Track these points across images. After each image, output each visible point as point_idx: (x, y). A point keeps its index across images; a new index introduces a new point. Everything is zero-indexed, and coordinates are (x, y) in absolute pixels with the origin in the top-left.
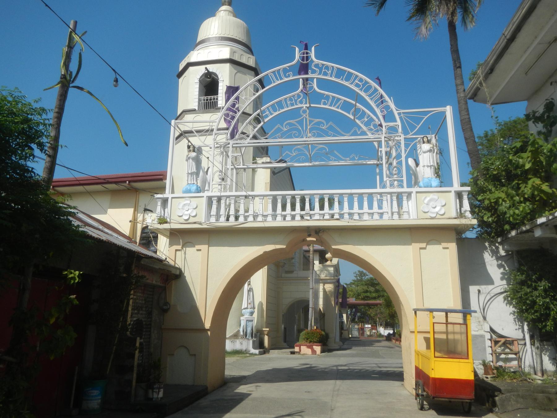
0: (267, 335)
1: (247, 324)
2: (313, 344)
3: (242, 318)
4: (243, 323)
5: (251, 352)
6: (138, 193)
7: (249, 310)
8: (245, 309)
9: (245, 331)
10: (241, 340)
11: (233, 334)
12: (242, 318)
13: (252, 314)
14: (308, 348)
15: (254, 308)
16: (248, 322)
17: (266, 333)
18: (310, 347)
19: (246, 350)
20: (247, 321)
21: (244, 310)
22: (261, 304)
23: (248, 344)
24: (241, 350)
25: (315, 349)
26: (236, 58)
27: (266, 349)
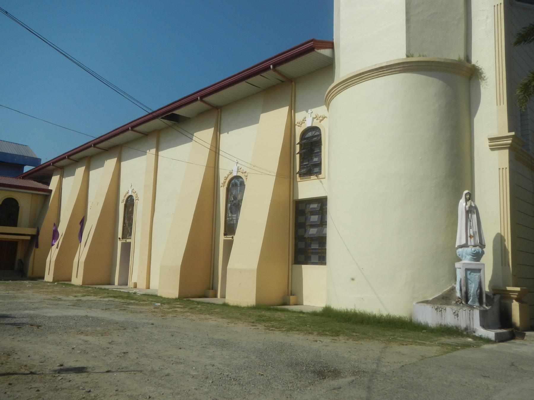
0: (517, 300)
1: (469, 277)
3: (457, 265)
4: (460, 274)
5: (478, 334)
6: (293, 83)
7: (470, 250)
8: (461, 247)
9: (464, 289)
10: (455, 308)
11: (440, 294)
12: (457, 265)
13: (477, 256)
15: (482, 245)
16: (469, 272)
17: (514, 296)
19: (466, 329)
20: (467, 270)
22: (499, 239)
23: (471, 318)
24: (457, 328)
27: (517, 328)
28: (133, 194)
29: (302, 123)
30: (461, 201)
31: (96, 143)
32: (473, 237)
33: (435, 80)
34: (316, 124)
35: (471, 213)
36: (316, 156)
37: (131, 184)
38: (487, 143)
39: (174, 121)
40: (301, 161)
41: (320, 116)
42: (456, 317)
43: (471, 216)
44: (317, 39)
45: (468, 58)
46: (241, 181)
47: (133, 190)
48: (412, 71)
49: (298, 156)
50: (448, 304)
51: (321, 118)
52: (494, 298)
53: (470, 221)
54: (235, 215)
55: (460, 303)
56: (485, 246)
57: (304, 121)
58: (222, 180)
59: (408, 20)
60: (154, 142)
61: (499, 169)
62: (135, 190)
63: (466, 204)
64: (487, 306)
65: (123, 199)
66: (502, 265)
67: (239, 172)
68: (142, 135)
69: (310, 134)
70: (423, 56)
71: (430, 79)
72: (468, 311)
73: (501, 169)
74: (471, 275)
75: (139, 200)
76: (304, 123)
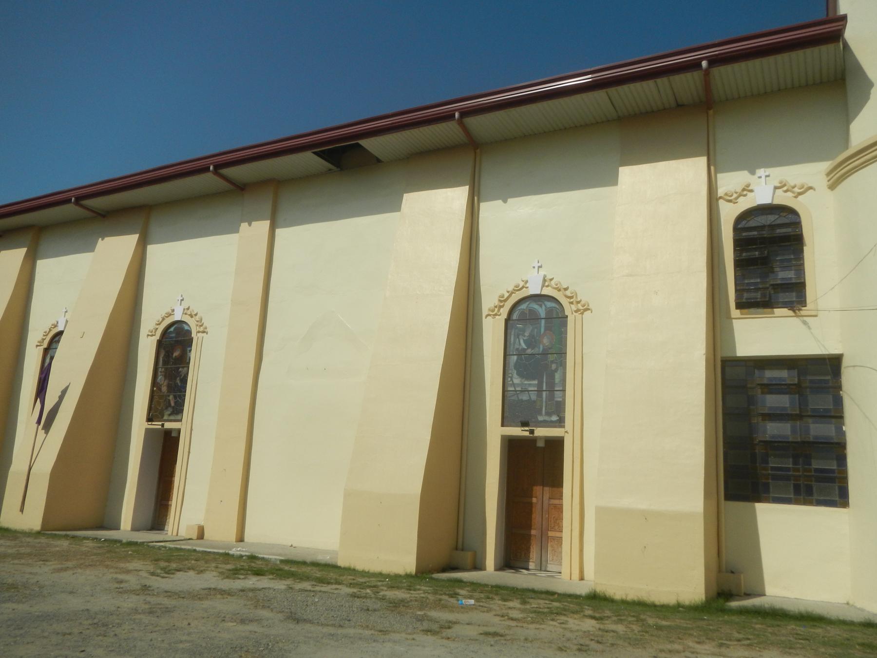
28: (186, 319)
29: (740, 195)
31: (81, 196)
37: (182, 296)
39: (332, 164)
46: (548, 306)
47: (188, 309)
54: (536, 382)
58: (488, 300)
60: (268, 207)
62: (195, 309)
65: (152, 328)
67: (547, 286)
68: (232, 187)
75: (207, 334)
76: (745, 195)
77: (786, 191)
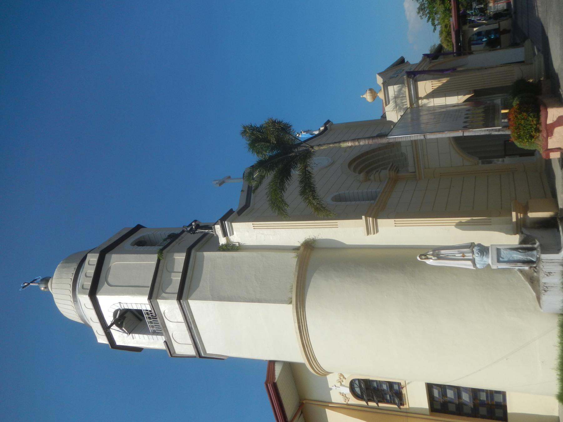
0: (525, 214)
1: (506, 259)
2: (543, 124)
6: (304, 402)
7: (477, 258)
8: (474, 264)
10: (542, 275)
11: (527, 283)
12: (494, 267)
13: (484, 250)
14: (552, 134)
15: (471, 246)
17: (521, 216)
18: (550, 130)
20: (499, 261)
21: (478, 266)
23: (552, 262)
25: (555, 119)
26: (88, 284)
29: (346, 397)
30: (428, 263)
32: (463, 254)
33: (312, 280)
34: (347, 383)
35: (439, 255)
36: (381, 386)
38: (372, 236)
40: (386, 401)
41: (339, 379)
42: (552, 274)
43: (443, 255)
44: (264, 379)
45: (296, 249)
48: (304, 300)
49: (381, 405)
50: (538, 280)
51: (342, 377)
52: (526, 235)
53: (448, 256)
55: (536, 269)
56: (472, 243)
57: (344, 394)
59: (259, 301)
61: (395, 226)
63: (431, 259)
64: (535, 244)
66: (491, 225)
69: (358, 390)
70: (292, 289)
71: (312, 284)
72: (544, 263)
73: (396, 225)
74: (504, 257)
76: (345, 395)
77: (343, 381)
